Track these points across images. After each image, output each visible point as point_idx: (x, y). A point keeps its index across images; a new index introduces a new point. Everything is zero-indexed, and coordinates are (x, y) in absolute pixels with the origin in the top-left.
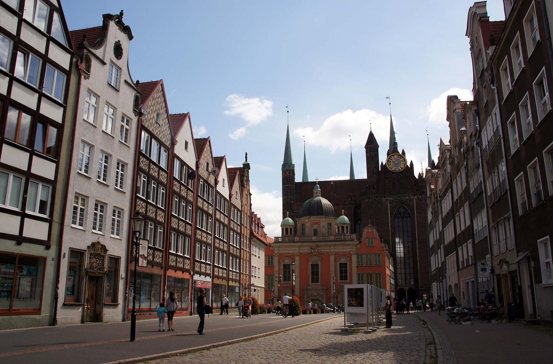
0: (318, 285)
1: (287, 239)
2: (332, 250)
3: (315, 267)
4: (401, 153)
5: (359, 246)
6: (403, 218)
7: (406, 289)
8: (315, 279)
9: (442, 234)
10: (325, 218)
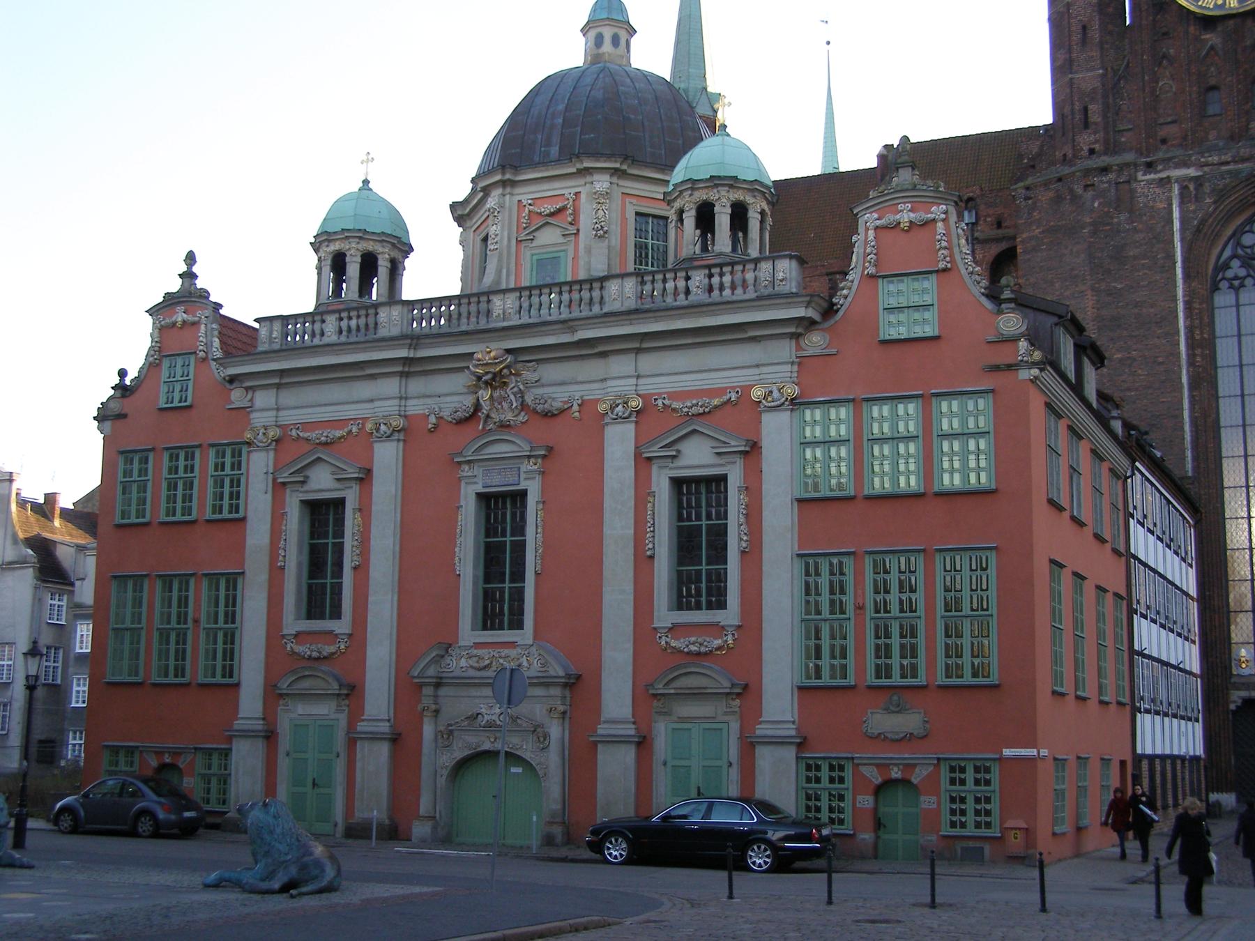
0: (523, 646)
1: (331, 324)
2: (619, 380)
3: (501, 508)
5: (816, 341)
8: (499, 609)
10: (615, 172)
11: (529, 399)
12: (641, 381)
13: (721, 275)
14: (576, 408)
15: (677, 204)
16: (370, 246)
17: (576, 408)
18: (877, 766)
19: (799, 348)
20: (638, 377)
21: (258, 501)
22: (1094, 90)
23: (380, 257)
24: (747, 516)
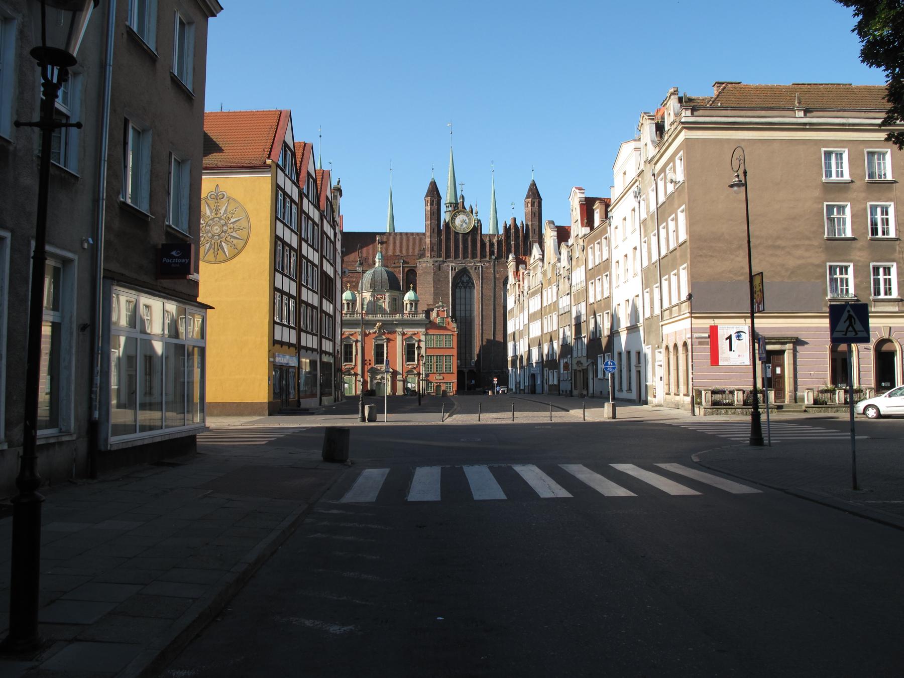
4: (468, 209)
6: (465, 288)
7: (466, 370)
9: (527, 326)
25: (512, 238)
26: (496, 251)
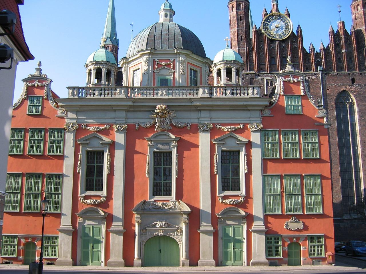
10: (187, 55)
11: (173, 122)
12: (212, 120)
13: (237, 90)
14: (189, 126)
15: (218, 67)
16: (110, 68)
17: (189, 126)
18: (289, 238)
19: (262, 114)
20: (211, 118)
21: (69, 150)
22: (244, 53)
23: (112, 71)
24: (247, 163)
25: (343, 45)
26: (323, 61)
